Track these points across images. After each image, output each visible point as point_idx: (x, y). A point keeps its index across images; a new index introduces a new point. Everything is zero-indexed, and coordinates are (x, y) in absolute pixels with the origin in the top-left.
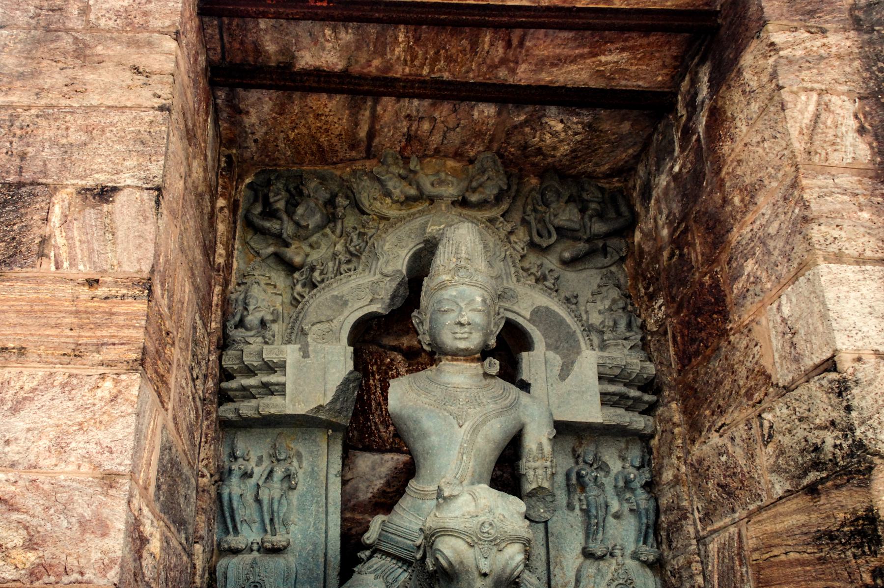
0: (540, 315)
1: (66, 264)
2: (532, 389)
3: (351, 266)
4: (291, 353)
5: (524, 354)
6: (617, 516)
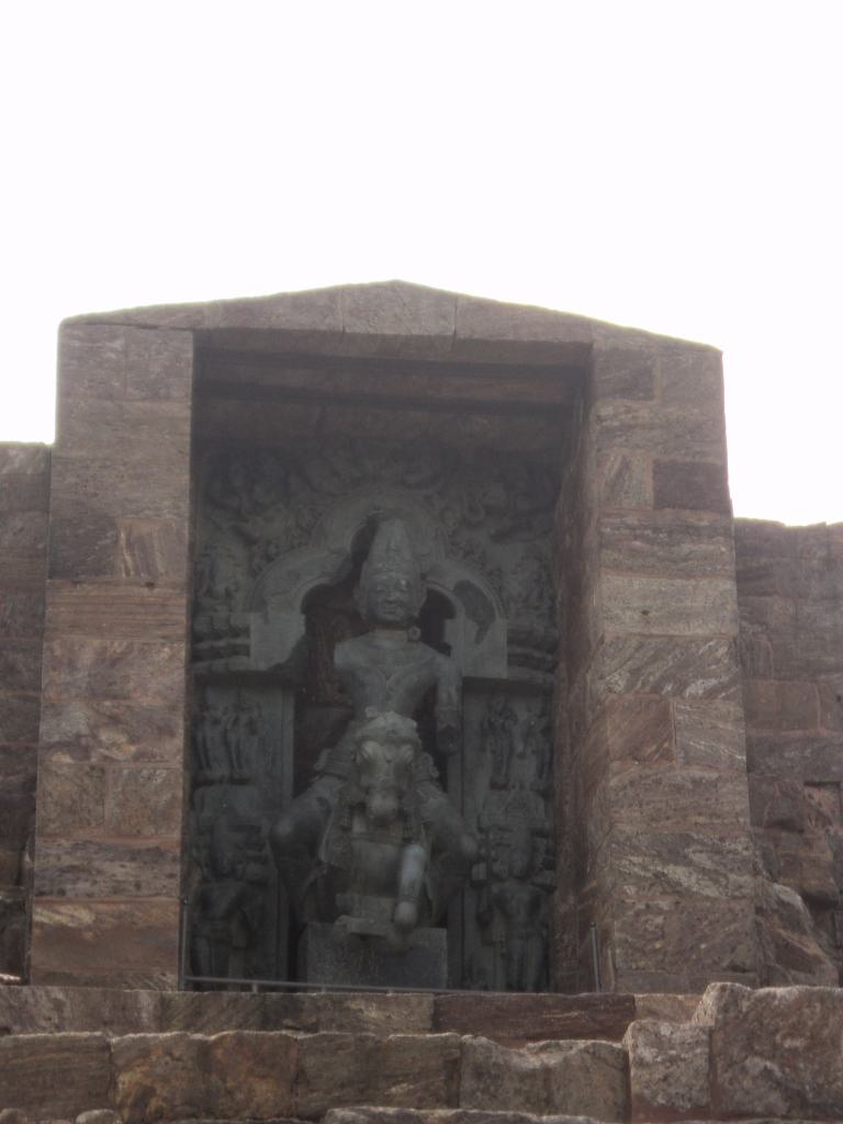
0: (463, 588)
1: (132, 573)
4: (254, 621)
5: (448, 623)
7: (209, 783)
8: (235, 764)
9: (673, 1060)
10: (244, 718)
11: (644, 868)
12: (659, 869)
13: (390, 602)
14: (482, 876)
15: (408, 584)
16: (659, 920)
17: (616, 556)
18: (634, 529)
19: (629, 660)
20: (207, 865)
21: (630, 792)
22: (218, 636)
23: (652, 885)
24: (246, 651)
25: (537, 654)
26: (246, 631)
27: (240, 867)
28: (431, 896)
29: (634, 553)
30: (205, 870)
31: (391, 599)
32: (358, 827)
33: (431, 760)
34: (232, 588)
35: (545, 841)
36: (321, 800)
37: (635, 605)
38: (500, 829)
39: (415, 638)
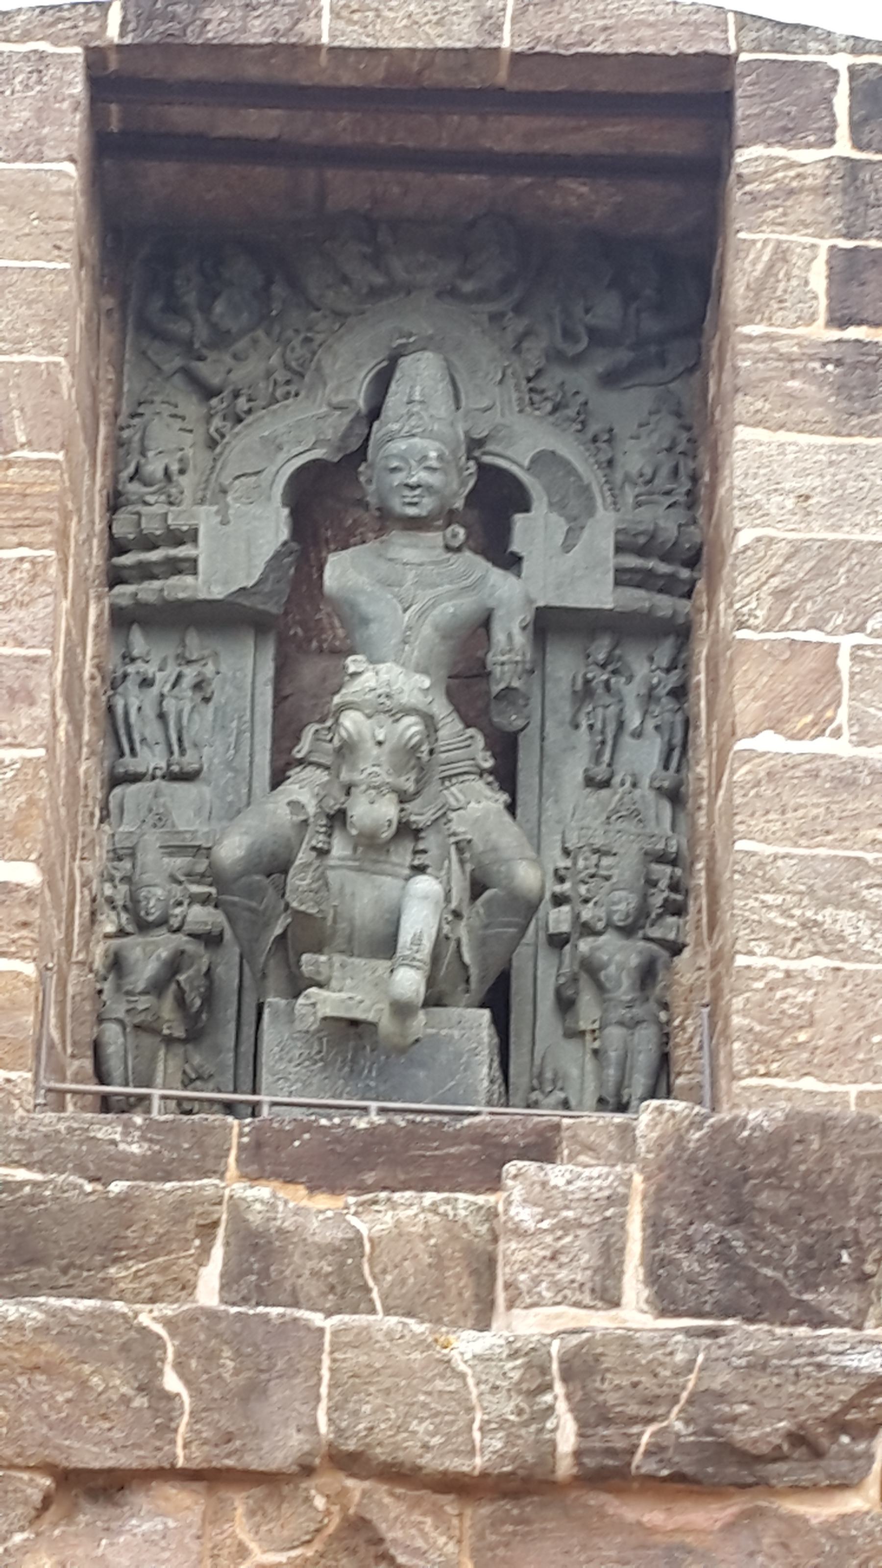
2: (525, 565)
3: (293, 388)
5: (519, 517)
6: (638, 734)
7: (135, 778)
8: (176, 748)
9: (566, 1226)
10: (190, 674)
11: (786, 913)
12: (809, 914)
13: (412, 488)
14: (565, 928)
15: (440, 457)
16: (807, 997)
17: (759, 404)
18: (792, 361)
19: (773, 576)
20: (125, 908)
21: (767, 790)
22: (151, 544)
23: (797, 940)
24: (190, 566)
25: (664, 568)
26: (192, 536)
27: (178, 911)
28: (467, 958)
29: (791, 399)
30: (124, 916)
31: (413, 480)
32: (339, 848)
33: (480, 741)
34: (175, 467)
35: (668, 869)
36: (295, 806)
37: (787, 486)
38: (596, 851)
39: (456, 544)
